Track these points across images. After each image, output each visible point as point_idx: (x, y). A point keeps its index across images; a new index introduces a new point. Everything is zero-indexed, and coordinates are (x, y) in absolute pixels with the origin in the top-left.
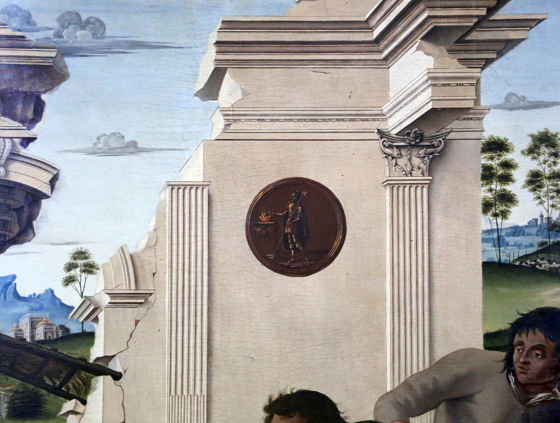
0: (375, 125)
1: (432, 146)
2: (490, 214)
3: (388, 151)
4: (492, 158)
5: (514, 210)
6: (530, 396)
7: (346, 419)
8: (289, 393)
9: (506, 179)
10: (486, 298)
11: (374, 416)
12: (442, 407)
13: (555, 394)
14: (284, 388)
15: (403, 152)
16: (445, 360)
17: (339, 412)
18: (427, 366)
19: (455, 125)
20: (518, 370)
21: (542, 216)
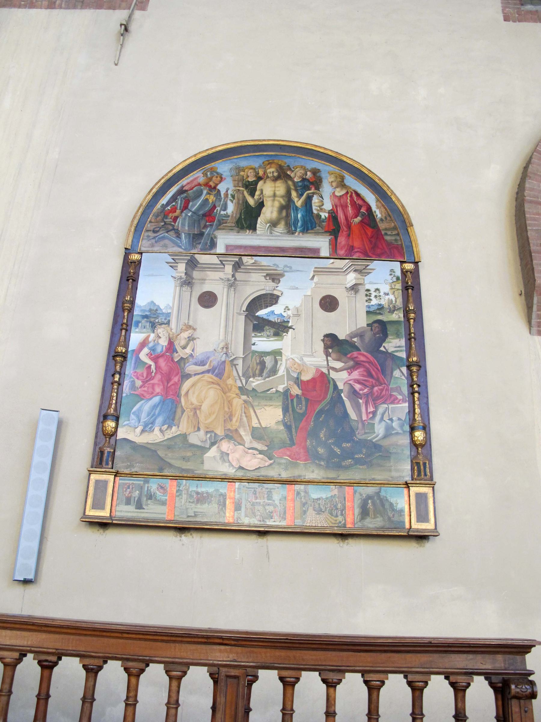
0: (344, 286)
5: (372, 302)
9: (370, 296)
10: (367, 318)
16: (359, 329)
19: (360, 286)
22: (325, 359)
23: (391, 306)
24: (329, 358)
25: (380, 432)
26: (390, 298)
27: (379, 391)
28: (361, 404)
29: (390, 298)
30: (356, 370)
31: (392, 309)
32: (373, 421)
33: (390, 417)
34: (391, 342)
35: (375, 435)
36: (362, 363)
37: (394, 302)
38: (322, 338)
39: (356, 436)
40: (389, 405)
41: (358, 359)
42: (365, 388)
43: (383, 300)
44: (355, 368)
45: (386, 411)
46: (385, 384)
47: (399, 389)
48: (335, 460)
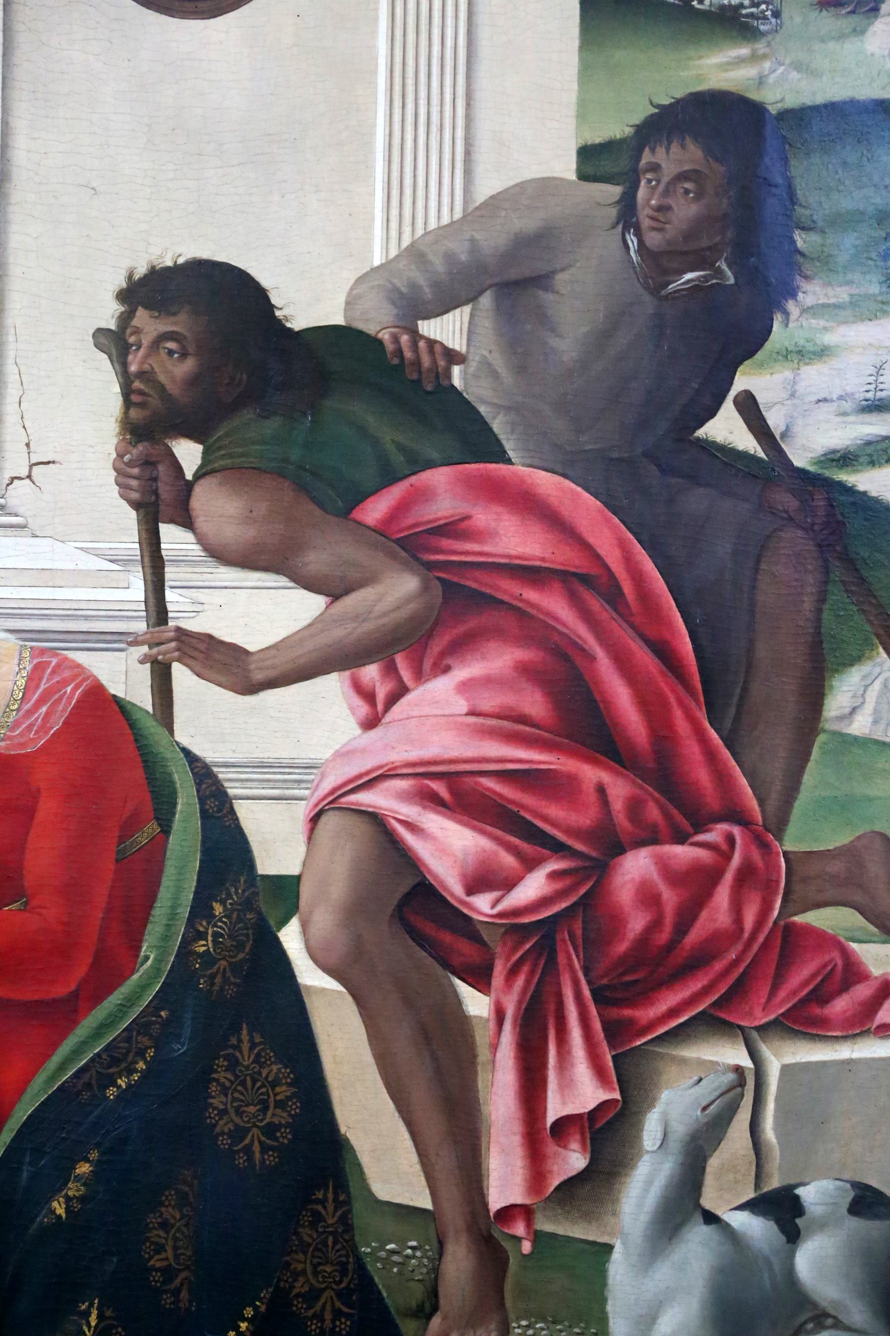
6: (670, 278)
7: (287, 321)
8: (170, 263)
10: (586, 71)
11: (345, 317)
12: (486, 300)
13: (719, 272)
14: (160, 253)
16: (494, 203)
17: (273, 306)
18: (458, 214)
20: (646, 223)
27: (669, 897)
28: (482, 1038)
30: (447, 669)
32: (588, 1217)
33: (774, 1183)
34: (822, 353)
40: (766, 1051)
42: (530, 864)
44: (436, 646)
45: (731, 1110)
46: (738, 816)
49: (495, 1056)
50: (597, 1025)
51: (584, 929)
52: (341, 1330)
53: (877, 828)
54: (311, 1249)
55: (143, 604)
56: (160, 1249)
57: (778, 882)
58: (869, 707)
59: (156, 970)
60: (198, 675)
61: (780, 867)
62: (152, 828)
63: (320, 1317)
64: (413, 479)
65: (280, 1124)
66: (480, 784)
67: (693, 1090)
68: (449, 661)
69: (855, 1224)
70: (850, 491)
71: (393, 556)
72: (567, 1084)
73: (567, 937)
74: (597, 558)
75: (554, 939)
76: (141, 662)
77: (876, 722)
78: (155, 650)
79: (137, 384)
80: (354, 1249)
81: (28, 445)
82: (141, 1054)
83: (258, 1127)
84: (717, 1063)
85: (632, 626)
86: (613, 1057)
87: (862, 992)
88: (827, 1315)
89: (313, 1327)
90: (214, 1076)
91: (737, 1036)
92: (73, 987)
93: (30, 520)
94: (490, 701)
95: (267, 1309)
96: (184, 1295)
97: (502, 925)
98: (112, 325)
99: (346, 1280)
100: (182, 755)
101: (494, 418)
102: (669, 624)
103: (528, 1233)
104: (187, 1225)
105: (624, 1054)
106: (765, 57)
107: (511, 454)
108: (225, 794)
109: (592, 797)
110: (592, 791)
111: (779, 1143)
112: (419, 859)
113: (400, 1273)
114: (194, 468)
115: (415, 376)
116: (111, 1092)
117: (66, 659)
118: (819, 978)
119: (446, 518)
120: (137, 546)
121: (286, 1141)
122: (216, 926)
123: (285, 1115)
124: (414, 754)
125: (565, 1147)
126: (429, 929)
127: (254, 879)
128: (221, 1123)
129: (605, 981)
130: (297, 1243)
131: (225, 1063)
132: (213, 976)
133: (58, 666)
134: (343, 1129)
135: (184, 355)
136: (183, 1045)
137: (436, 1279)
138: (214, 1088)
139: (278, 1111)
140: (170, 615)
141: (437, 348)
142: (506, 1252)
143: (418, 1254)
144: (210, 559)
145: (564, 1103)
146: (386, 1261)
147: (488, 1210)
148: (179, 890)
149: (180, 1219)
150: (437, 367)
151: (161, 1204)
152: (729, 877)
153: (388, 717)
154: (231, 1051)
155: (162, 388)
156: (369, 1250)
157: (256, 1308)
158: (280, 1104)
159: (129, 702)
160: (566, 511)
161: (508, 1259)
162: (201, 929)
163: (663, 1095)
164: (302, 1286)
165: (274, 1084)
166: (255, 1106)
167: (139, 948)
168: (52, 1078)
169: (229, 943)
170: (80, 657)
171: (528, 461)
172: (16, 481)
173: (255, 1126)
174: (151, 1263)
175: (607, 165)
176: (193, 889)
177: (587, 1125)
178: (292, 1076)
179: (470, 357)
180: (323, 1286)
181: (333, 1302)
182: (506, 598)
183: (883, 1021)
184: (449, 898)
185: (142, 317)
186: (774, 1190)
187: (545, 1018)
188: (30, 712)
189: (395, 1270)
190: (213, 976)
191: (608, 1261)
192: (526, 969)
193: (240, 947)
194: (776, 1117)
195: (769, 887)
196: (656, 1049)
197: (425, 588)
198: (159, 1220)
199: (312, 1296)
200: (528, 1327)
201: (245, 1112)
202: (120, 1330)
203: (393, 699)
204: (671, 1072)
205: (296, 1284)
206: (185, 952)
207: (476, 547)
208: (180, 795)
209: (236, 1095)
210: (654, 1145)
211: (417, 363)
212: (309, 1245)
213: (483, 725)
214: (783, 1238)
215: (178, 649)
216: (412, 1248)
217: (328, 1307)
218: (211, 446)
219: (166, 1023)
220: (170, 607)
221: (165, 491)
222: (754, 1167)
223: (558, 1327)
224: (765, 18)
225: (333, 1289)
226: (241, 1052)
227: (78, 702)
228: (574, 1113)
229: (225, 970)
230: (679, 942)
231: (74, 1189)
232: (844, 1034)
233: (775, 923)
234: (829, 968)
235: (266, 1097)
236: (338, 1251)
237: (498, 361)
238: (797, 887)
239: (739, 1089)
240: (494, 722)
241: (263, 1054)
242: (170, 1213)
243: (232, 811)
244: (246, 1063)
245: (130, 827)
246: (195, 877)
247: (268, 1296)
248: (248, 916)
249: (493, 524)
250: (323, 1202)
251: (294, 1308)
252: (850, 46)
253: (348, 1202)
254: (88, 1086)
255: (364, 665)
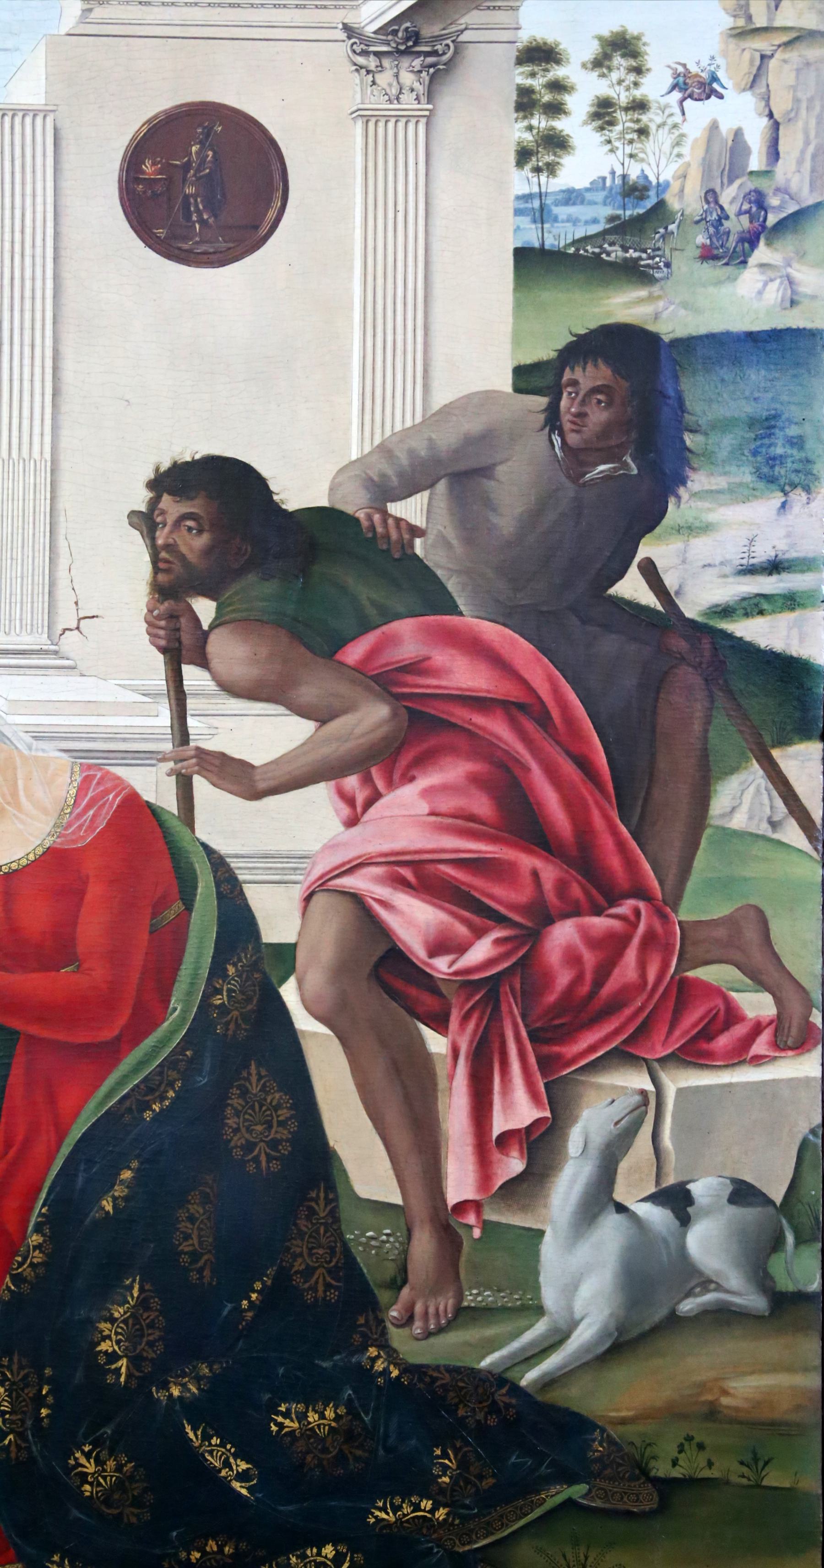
1: (434, 53)
2: (528, 167)
3: (361, 60)
4: (533, 75)
8: (189, 459)
9: (556, 109)
10: (518, 306)
11: (329, 501)
12: (441, 486)
13: (625, 465)
15: (386, 63)
16: (447, 410)
18: (419, 419)
20: (567, 426)
21: (613, 173)
22: (158, 679)
23: (729, 197)
24: (193, 675)
25: (578, 1313)
26: (726, 128)
27: (589, 958)
28: (442, 1070)
29: (726, 128)
30: (412, 779)
31: (737, 225)
32: (524, 1209)
33: (670, 1180)
34: (706, 528)
35: (540, 1328)
36: (461, 715)
37: (756, 162)
38: (140, 499)
39: (384, 1345)
40: (665, 1077)
41: (428, 684)
42: (479, 933)
43: (660, 140)
44: (403, 762)
47: (751, 934)
48: (212, 1546)
49: (451, 1084)
50: (532, 1060)
51: (522, 984)
52: (331, 1299)
53: (752, 901)
54: (307, 1236)
55: (169, 729)
56: (187, 1237)
57: (674, 945)
58: (745, 808)
59: (183, 1018)
60: (214, 785)
61: (675, 934)
62: (178, 906)
63: (314, 1289)
64: (384, 628)
65: (282, 1140)
66: (439, 870)
67: (607, 1109)
68: (415, 772)
69: (732, 1210)
70: (729, 636)
71: (368, 689)
72: (508, 1106)
73: (508, 990)
74: (530, 689)
75: (498, 991)
76: (169, 775)
77: (751, 818)
78: (179, 765)
79: (163, 555)
80: (341, 1235)
81: (76, 603)
82: (171, 1085)
83: (264, 1141)
84: (626, 1088)
85: (558, 743)
86: (547, 1085)
87: (739, 1030)
88: (711, 1281)
89: (309, 1297)
90: (229, 1101)
91: (642, 1066)
92: (116, 1032)
93: (78, 662)
94: (447, 804)
95: (272, 1283)
96: (207, 1273)
97: (455, 981)
98: (143, 508)
99: (335, 1260)
100: (201, 849)
101: (449, 579)
102: (588, 742)
103: (478, 1222)
104: (209, 1219)
105: (553, 1081)
106: (659, 298)
107: (462, 608)
108: (236, 879)
109: (528, 879)
110: (528, 874)
111: (675, 1149)
112: (390, 929)
113: (377, 1254)
114: (210, 620)
115: (385, 547)
116: (148, 1115)
117: (108, 772)
118: (706, 1020)
119: (411, 658)
120: (164, 682)
121: (286, 1153)
122: (229, 983)
123: (285, 1132)
124: (386, 847)
125: (507, 1155)
126: (399, 984)
127: (260, 946)
128: (235, 1138)
129: (538, 1025)
130: (295, 1232)
131: (238, 1092)
132: (227, 1024)
133: (102, 778)
134: (331, 1143)
135: (200, 531)
136: (204, 1078)
137: (406, 1260)
138: (229, 1111)
139: (280, 1129)
140: (191, 737)
141: (403, 525)
142: (460, 1237)
143: (392, 1239)
144: (222, 693)
145: (506, 1121)
146: (366, 1245)
147: (446, 1205)
148: (199, 956)
149: (204, 1214)
150: (403, 539)
151: (189, 1202)
152: (636, 941)
153: (366, 817)
154: (243, 1082)
155: (182, 558)
156: (352, 1237)
157: (264, 1283)
158: (281, 1124)
159: (159, 807)
160: (506, 652)
161: (462, 1243)
162: (218, 986)
163: (584, 1114)
164: (300, 1265)
165: (277, 1108)
166: (262, 1125)
167: (169, 1001)
168: (102, 1103)
169: (240, 997)
170: (120, 771)
171: (476, 614)
172: (67, 632)
173: (262, 1141)
174: (181, 1248)
175: (537, 381)
176: (211, 954)
177: (524, 1137)
178: (291, 1101)
179: (429, 531)
180: (317, 1265)
181: (324, 1277)
182: (459, 723)
183: (755, 1053)
184: (415, 960)
185: (166, 501)
186: (672, 1185)
187: (492, 1053)
188: (80, 816)
189: (373, 1252)
190: (227, 1024)
191: (540, 1243)
192: (476, 1016)
193: (249, 1000)
194: (672, 1129)
195: (668, 949)
196: (578, 1077)
197: (395, 714)
198: (187, 1215)
199: (309, 1272)
200: (478, 1295)
201: (253, 1130)
202: (156, 1300)
203: (369, 803)
204: (590, 1095)
205: (295, 1264)
206: (205, 1005)
207: (434, 682)
208: (200, 880)
209: (247, 1116)
210: (577, 1152)
211: (387, 536)
212: (306, 1233)
213: (441, 823)
214: (677, 1223)
215: (198, 764)
216: (387, 1235)
217: (321, 1280)
218: (223, 603)
219: (191, 1061)
220: (191, 731)
221: (187, 638)
222: (655, 1169)
223: (502, 1294)
224: (659, 268)
225: (324, 1267)
226: (251, 1084)
227: (118, 806)
228: (515, 1128)
229: (236, 1019)
230: (597, 993)
231: (119, 1191)
232: (726, 1063)
233: (672, 977)
234: (714, 1012)
235: (269, 1118)
236: (328, 1238)
237: (451, 534)
238: (689, 948)
239: (643, 1108)
240: (450, 821)
241: (268, 1084)
242: (196, 1209)
243: (242, 893)
244: (254, 1092)
245: (161, 905)
246: (213, 945)
247: (273, 1273)
248: (256, 976)
249: (448, 664)
250: (316, 1200)
251: (294, 1283)
252: (726, 290)
253: (336, 1199)
254: (129, 1110)
255: (346, 776)
